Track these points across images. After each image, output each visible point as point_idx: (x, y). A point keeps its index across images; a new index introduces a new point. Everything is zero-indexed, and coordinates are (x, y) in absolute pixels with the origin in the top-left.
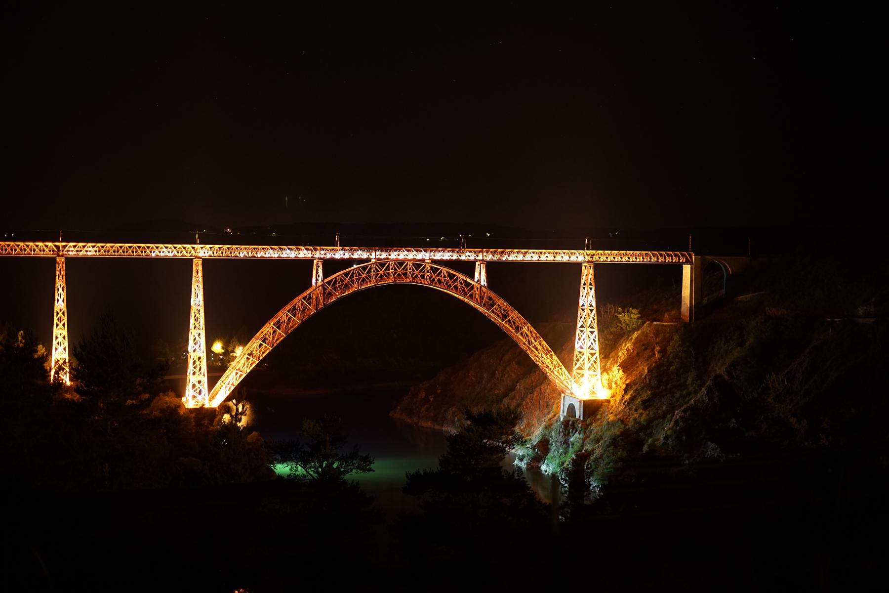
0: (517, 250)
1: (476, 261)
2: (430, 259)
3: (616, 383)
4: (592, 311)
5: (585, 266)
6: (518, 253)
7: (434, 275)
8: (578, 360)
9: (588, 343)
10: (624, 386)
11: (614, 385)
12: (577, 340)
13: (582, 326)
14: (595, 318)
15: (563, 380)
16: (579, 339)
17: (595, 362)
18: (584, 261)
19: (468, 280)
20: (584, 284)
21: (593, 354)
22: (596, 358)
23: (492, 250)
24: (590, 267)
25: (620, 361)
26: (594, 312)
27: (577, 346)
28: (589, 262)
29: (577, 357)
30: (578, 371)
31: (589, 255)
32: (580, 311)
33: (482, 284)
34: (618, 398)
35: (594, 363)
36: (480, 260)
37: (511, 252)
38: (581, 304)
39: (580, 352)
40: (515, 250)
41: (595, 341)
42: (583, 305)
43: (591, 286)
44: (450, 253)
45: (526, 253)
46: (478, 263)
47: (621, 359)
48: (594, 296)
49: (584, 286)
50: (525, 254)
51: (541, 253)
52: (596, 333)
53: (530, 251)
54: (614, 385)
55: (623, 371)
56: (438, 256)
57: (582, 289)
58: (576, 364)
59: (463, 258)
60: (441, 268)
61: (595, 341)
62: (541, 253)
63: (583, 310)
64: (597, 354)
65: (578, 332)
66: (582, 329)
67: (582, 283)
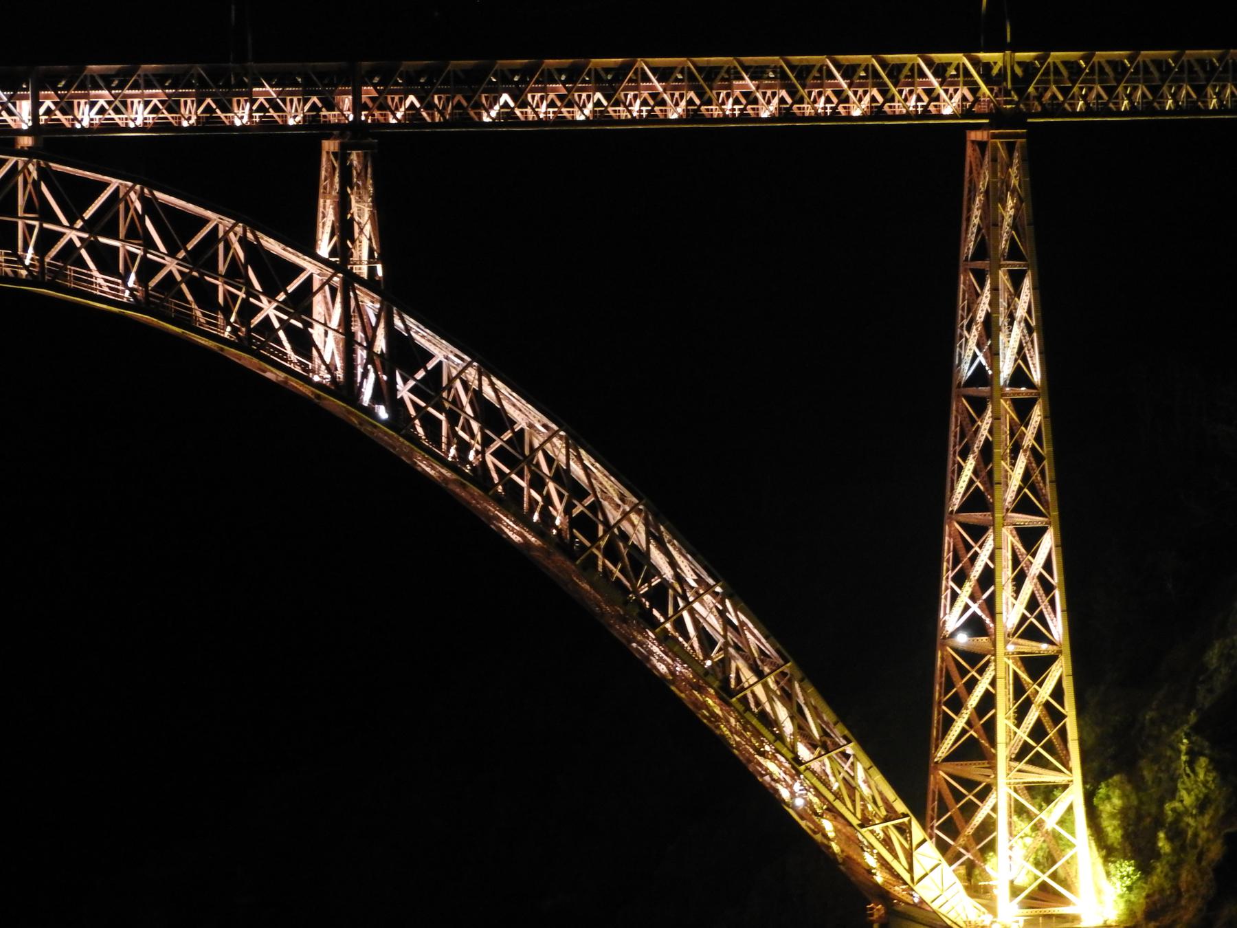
0: (566, 62)
1: (315, 129)
2: (35, 130)
3: (1176, 834)
4: (1023, 408)
5: (982, 145)
6: (573, 75)
7: (72, 222)
8: (957, 704)
9: (1011, 611)
10: (1215, 851)
11: (1163, 844)
12: (947, 583)
13: (977, 501)
14: (1045, 451)
15: (855, 822)
16: (960, 579)
17: (1057, 717)
18: (967, 113)
19: (273, 246)
20: (982, 251)
21: (1037, 666)
22: (1058, 693)
23: (408, 65)
24: (1010, 148)
25: (1205, 699)
26: (1037, 416)
27: (951, 619)
28: (998, 118)
29: (949, 684)
30: (956, 768)
31: (1002, 74)
32: (960, 406)
33: (363, 271)
34: (1189, 911)
35: (1047, 721)
36: (340, 130)
37: (527, 73)
38: (966, 371)
39: (973, 657)
40: (550, 62)
41: (1047, 587)
42: (980, 376)
43: (1016, 265)
44: (157, 95)
45: (619, 74)
46: (330, 146)
47: (1210, 691)
48: (1033, 323)
49: (979, 264)
50: (610, 85)
51: (711, 74)
52: (1048, 543)
53: (641, 63)
54: (1163, 844)
55: (1217, 765)
56: (86, 116)
57: (966, 280)
58: (948, 723)
59: (241, 116)
60: (115, 183)
61: (1047, 587)
62: (711, 74)
63: (980, 405)
64: (1060, 670)
65: (952, 532)
66: (976, 517)
67: (969, 247)
